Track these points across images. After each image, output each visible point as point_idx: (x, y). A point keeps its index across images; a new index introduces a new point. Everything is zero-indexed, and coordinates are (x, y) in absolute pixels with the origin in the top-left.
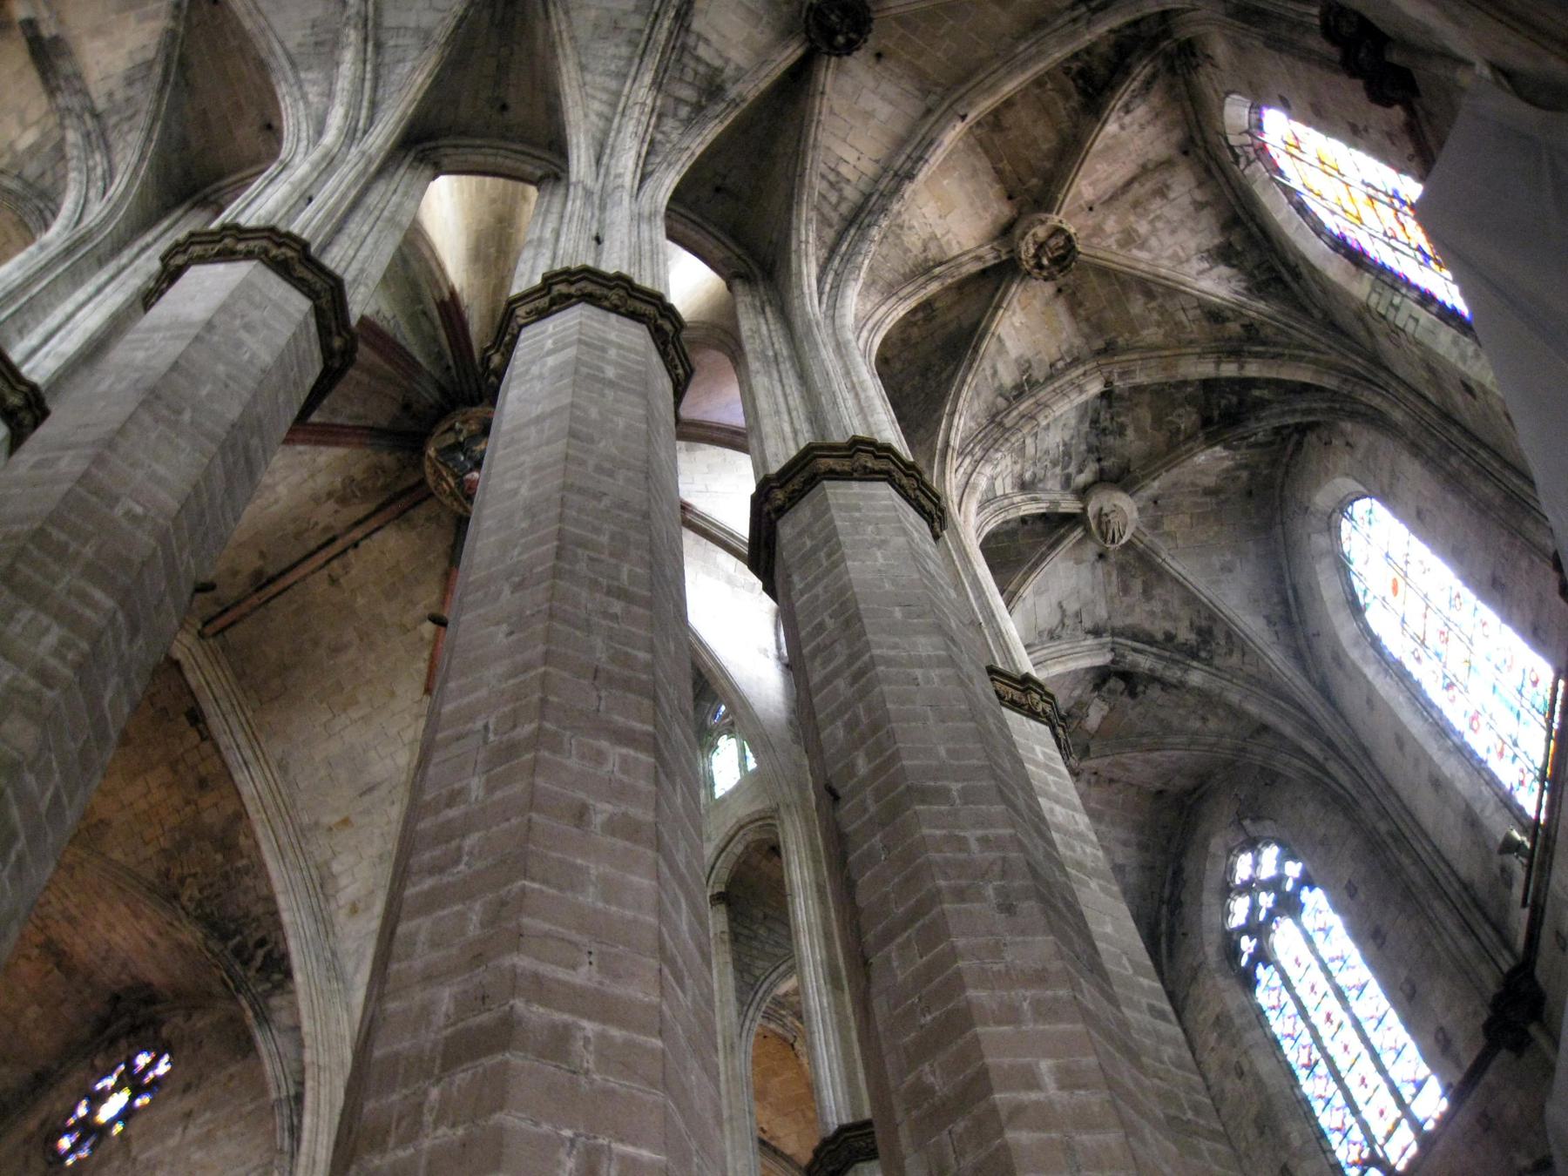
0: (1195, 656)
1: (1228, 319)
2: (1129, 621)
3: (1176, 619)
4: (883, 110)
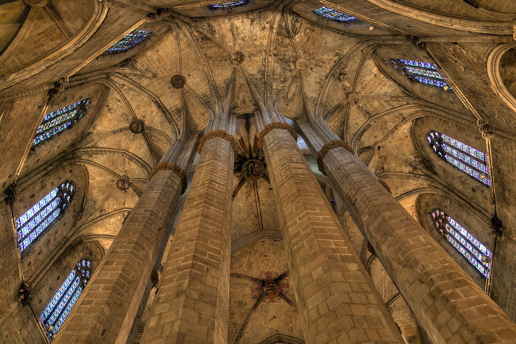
0: (342, 58)
1: (265, 26)
2: (328, 69)
3: (332, 59)
4: (198, 79)
